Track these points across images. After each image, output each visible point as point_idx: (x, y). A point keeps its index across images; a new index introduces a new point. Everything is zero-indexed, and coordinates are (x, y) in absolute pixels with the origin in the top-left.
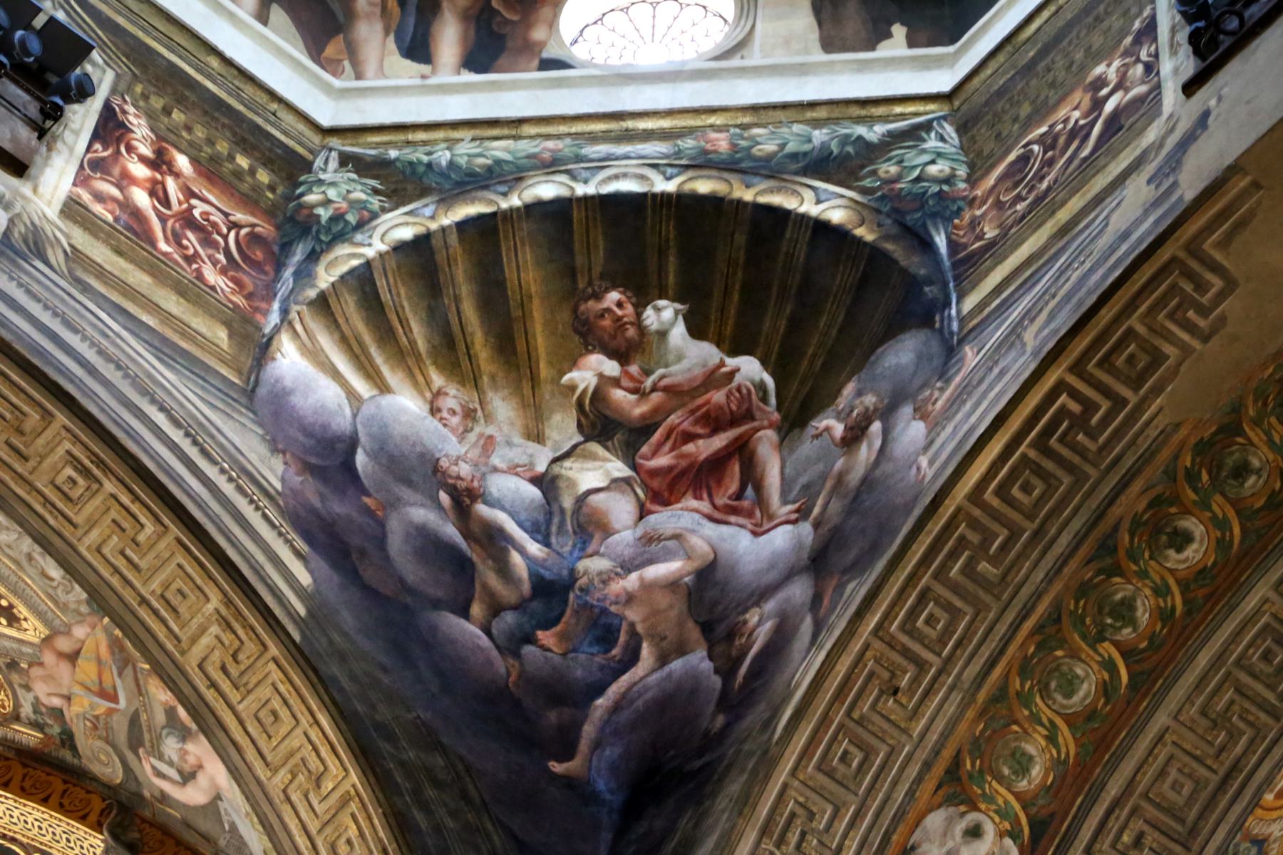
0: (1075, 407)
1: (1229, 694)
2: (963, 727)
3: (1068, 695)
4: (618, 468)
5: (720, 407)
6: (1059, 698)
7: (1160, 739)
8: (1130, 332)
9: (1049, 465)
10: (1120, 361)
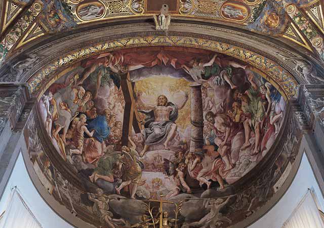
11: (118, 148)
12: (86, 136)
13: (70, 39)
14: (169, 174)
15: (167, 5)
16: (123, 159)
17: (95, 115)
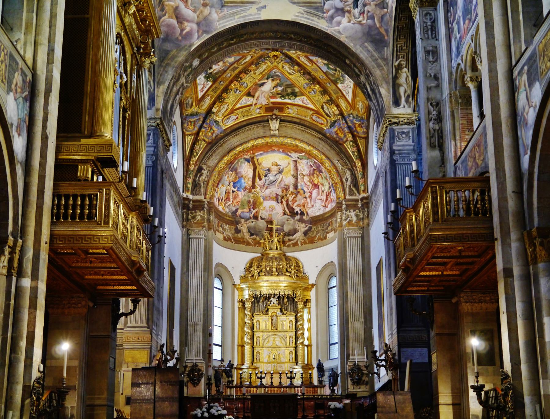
11: (250, 191)
12: (233, 192)
13: (221, 146)
14: (278, 203)
16: (253, 197)
17: (237, 179)
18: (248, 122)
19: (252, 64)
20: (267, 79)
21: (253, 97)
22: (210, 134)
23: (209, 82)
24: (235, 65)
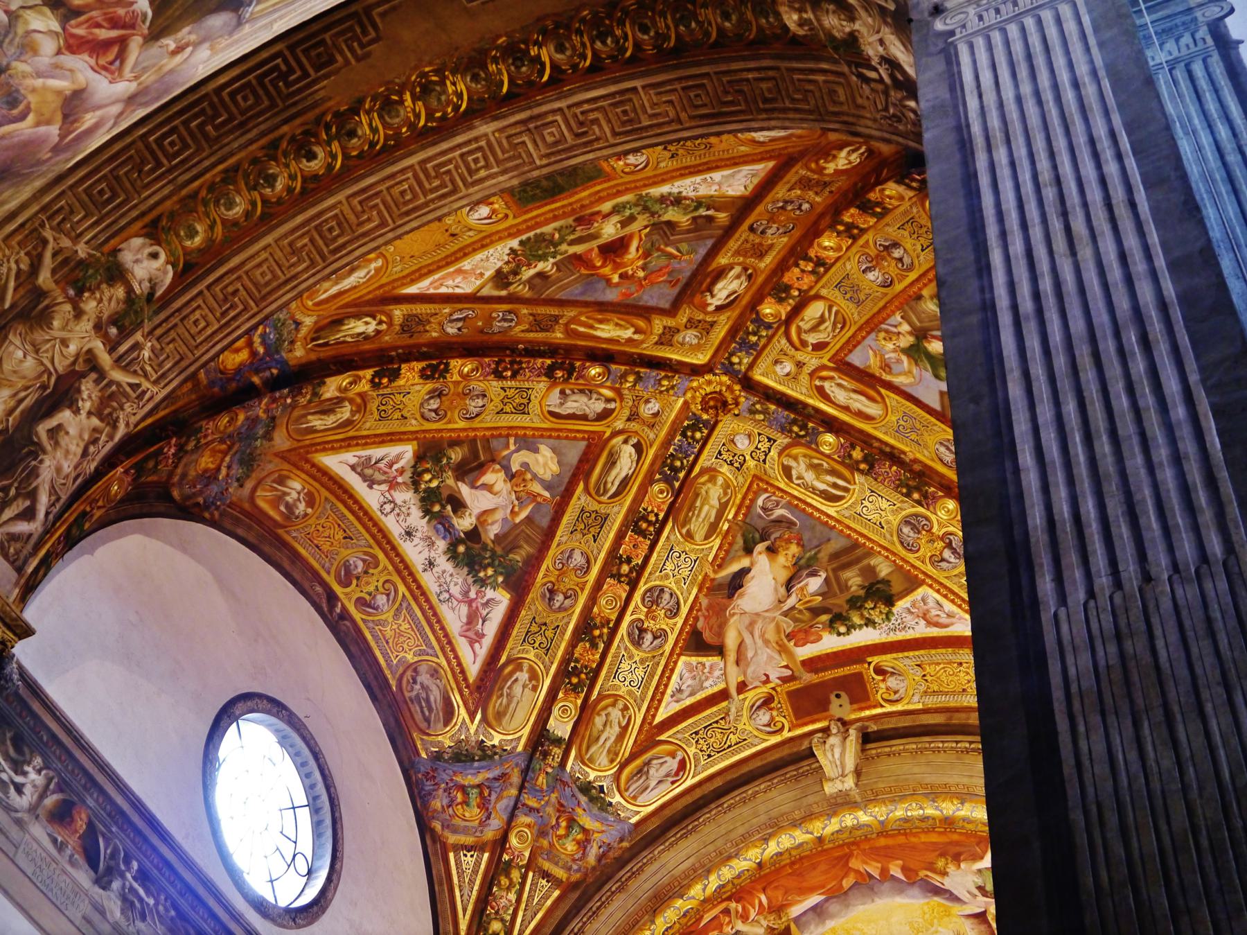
0: (283, 68)
1: (306, 240)
2: (168, 203)
3: (228, 209)
4: (55, 25)
5: (120, 17)
6: (222, 208)
7: (265, 248)
8: (323, 42)
9: (261, 92)
10: (313, 53)
13: (620, 889)
15: (843, 694)
18: (729, 776)
19: (649, 481)
20: (748, 550)
21: (720, 650)
22: (571, 847)
23: (490, 593)
24: (580, 499)
